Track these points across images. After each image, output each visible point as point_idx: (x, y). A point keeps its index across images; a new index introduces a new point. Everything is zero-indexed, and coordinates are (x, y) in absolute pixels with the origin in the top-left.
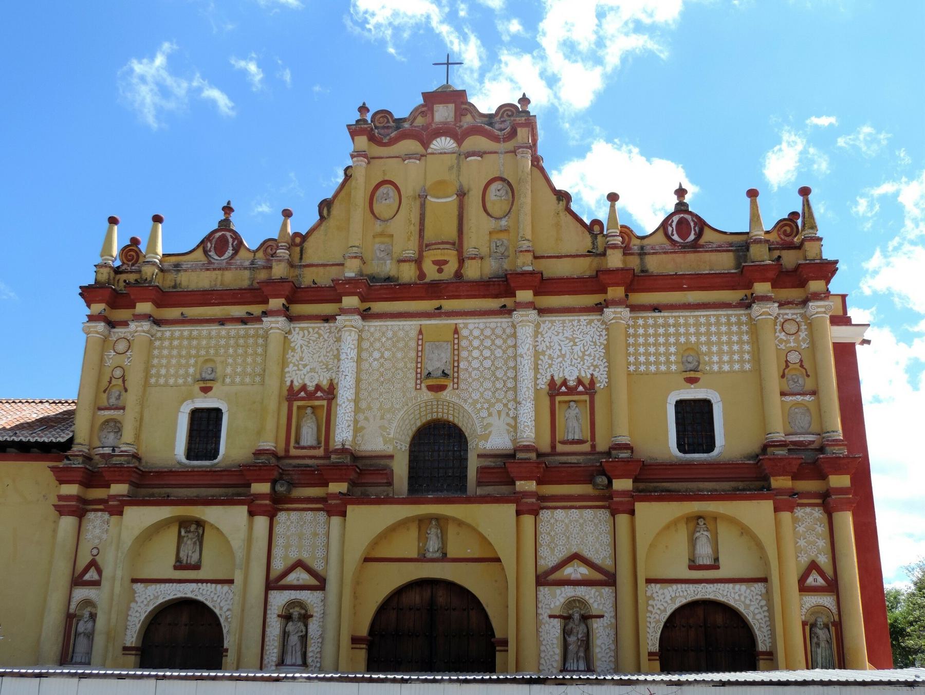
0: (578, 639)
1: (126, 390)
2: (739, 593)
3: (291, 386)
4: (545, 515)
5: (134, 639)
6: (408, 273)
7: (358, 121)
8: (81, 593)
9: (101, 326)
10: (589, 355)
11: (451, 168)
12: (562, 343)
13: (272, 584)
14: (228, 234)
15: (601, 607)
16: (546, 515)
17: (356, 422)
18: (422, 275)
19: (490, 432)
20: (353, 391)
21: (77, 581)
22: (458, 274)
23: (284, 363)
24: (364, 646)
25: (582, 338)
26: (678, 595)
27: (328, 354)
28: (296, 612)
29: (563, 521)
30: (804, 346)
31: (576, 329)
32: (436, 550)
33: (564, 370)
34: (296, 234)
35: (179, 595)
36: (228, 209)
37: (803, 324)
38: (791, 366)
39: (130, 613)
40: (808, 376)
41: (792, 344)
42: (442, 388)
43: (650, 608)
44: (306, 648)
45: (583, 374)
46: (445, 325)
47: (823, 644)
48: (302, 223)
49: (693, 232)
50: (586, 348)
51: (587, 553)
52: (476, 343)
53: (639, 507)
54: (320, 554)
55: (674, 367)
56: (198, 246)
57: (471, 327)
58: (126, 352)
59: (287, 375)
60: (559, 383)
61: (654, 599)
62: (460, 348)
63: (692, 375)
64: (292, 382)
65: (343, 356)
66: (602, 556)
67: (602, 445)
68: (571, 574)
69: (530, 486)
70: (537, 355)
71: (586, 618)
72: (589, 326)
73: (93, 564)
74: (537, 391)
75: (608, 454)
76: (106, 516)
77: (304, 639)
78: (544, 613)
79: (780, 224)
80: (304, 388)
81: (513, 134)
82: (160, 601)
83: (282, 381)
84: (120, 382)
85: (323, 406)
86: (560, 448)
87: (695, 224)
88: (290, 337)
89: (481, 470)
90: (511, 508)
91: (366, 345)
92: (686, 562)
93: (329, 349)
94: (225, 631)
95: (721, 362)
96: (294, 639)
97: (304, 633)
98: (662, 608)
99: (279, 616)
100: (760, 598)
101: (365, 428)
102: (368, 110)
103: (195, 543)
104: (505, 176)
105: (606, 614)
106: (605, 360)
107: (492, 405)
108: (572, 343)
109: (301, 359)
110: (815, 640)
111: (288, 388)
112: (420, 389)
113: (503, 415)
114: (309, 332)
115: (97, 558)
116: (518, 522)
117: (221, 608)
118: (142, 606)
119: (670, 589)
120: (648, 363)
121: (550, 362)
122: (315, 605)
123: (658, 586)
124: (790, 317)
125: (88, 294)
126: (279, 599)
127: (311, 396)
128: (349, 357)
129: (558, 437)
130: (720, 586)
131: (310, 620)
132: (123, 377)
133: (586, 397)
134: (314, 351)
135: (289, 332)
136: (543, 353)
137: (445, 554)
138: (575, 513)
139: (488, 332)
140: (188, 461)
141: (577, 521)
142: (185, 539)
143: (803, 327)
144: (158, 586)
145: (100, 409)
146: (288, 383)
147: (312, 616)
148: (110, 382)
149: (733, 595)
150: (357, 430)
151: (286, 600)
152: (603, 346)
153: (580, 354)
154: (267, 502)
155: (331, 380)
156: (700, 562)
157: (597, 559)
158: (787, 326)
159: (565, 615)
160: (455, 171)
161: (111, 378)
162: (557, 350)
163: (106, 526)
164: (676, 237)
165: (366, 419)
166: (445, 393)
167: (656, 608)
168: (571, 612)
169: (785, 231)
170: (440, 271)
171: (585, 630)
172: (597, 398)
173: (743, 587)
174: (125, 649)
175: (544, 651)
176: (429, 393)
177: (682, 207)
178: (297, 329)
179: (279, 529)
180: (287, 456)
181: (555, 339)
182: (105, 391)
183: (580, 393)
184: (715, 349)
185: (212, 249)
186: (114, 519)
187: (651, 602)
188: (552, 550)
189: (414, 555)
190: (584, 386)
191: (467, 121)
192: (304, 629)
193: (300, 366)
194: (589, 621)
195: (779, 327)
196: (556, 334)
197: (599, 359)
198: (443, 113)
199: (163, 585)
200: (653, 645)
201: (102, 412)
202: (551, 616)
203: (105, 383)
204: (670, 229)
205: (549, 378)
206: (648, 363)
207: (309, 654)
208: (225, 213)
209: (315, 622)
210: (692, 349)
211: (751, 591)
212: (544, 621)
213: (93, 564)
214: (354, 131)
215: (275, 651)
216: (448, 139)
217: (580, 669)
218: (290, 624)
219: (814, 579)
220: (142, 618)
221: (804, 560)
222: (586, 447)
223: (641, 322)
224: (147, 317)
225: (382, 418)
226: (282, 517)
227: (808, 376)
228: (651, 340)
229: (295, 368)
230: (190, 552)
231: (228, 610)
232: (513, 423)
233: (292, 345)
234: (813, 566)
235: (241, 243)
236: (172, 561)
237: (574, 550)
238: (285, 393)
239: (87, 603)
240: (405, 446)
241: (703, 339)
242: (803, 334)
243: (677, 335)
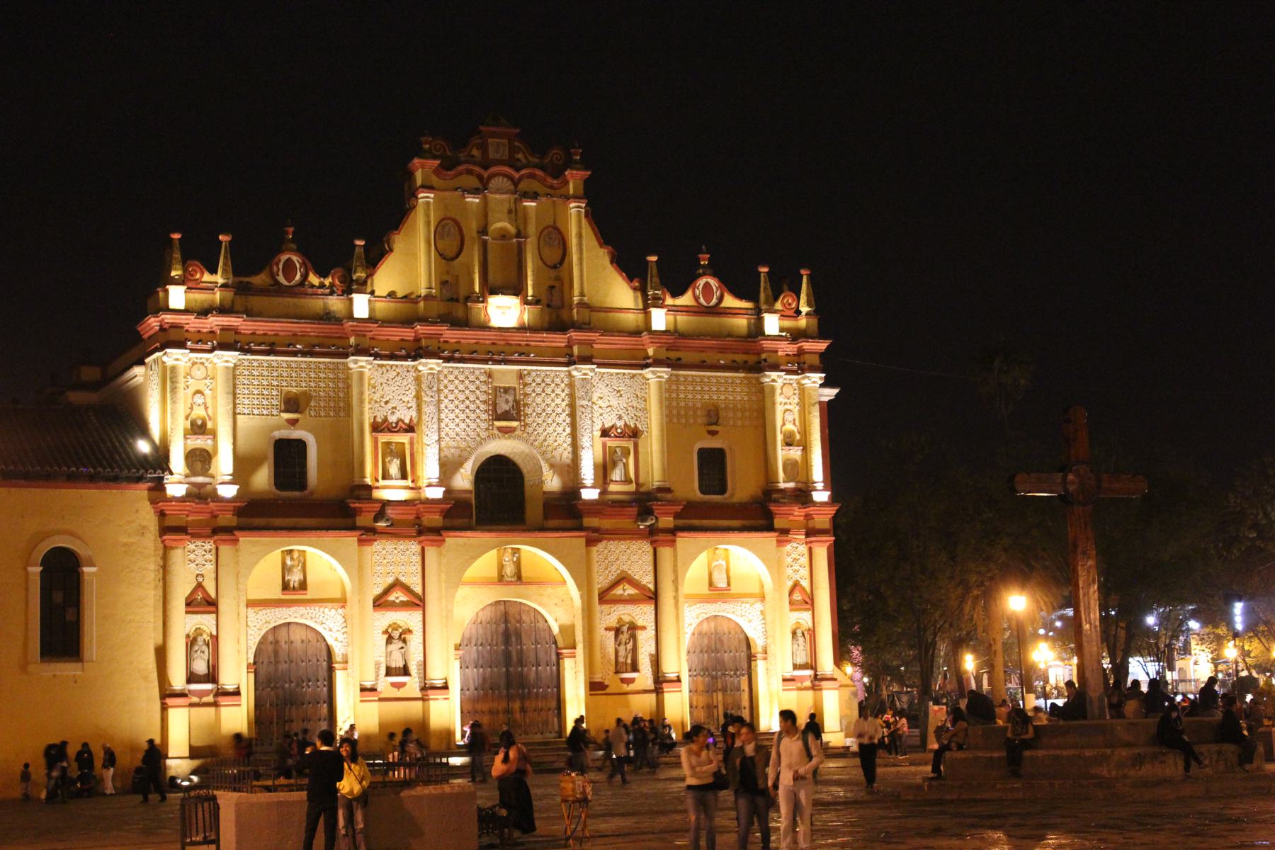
11: (510, 212)
14: (295, 258)
20: (437, 434)
27: (407, 393)
46: (512, 371)
49: (715, 297)
54: (418, 579)
63: (714, 428)
108: (618, 395)
118: (255, 629)
140: (278, 492)
147: (410, 631)
148: (192, 408)
160: (513, 215)
161: (192, 405)
164: (702, 300)
185: (280, 273)
193: (383, 404)
204: (697, 292)
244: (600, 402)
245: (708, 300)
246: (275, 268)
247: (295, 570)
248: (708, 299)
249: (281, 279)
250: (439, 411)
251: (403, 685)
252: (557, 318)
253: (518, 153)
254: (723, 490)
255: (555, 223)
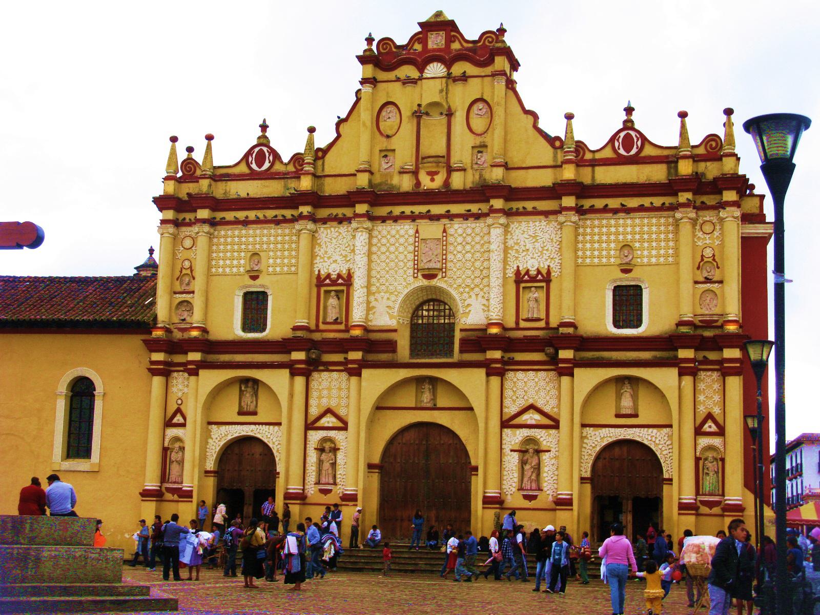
0: (532, 467)
1: (194, 278)
2: (652, 435)
3: (319, 275)
4: (510, 375)
5: (212, 465)
6: (406, 184)
7: (365, 51)
8: (172, 432)
9: (171, 229)
10: (547, 250)
11: (441, 91)
12: (526, 241)
13: (310, 426)
14: (265, 149)
15: (548, 444)
16: (510, 375)
17: (368, 302)
18: (418, 184)
19: (470, 311)
21: (169, 423)
22: (447, 183)
23: (313, 256)
24: (377, 471)
25: (542, 237)
26: (605, 436)
27: (346, 249)
28: (327, 445)
29: (523, 380)
30: (717, 242)
31: (538, 229)
32: (429, 401)
33: (527, 262)
34: (319, 149)
35: (243, 433)
36: (264, 127)
37: (718, 225)
38: (706, 260)
39: (208, 447)
40: (718, 268)
41: (708, 242)
42: (433, 276)
43: (584, 445)
44: (335, 472)
45: (542, 266)
47: (711, 474)
48: (322, 140)
49: (635, 146)
50: (545, 244)
51: (539, 404)
52: (460, 240)
53: (577, 371)
55: (612, 260)
56: (242, 160)
57: (456, 226)
58: (192, 247)
59: (316, 266)
60: (523, 273)
61: (588, 439)
62: (448, 244)
64: (319, 271)
65: (357, 252)
66: (551, 407)
67: (554, 323)
68: (527, 419)
69: (497, 354)
70: (506, 250)
71: (538, 452)
72: (548, 226)
73: (178, 411)
74: (505, 278)
75: (557, 329)
76: (186, 375)
77: (334, 465)
78: (507, 448)
79: (708, 139)
80: (328, 276)
81: (490, 61)
82: (229, 437)
83: (312, 272)
84: (189, 272)
85: (343, 291)
86: (523, 324)
87: (638, 140)
88: (316, 235)
89: (463, 341)
90: (482, 372)
91: (375, 241)
92: (613, 412)
93: (346, 245)
94: (277, 459)
95: (650, 256)
96: (326, 465)
97: (334, 461)
98: (593, 445)
99: (315, 449)
100: (666, 438)
101: (375, 307)
102: (373, 40)
103: (252, 396)
104: (485, 98)
105: (552, 449)
106: (559, 254)
107: (473, 289)
109: (326, 252)
110: (706, 471)
111: (316, 276)
112: (417, 277)
113: (480, 297)
114: (331, 232)
115: (182, 407)
116: (488, 382)
117: (274, 443)
118: (217, 441)
119: (600, 431)
120: (592, 257)
121: (516, 255)
122: (341, 441)
123: (592, 429)
124: (708, 219)
125: (161, 202)
126: (315, 437)
127: (334, 283)
128: (362, 252)
129: (524, 314)
130: (637, 430)
131: (338, 452)
132: (191, 267)
133: (544, 284)
134: (336, 247)
135: (316, 231)
136: (512, 248)
137: (435, 405)
138: (531, 374)
139: (469, 231)
141: (533, 380)
142: (245, 393)
143: (718, 227)
144: (227, 426)
145: (175, 293)
146: (317, 273)
147: (339, 449)
148: (181, 272)
149: (646, 436)
150: (369, 309)
151: (320, 437)
152: (558, 243)
153: (540, 249)
154: (303, 366)
155: (349, 270)
156: (623, 412)
157: (547, 409)
158: (704, 228)
159: (523, 449)
160: (444, 93)
161: (181, 269)
162: (522, 246)
163: (186, 383)
164: (622, 151)
165: (376, 300)
166: (435, 280)
167: (589, 445)
168: (527, 447)
169: (711, 145)
170: (432, 180)
171: (537, 461)
172: (552, 285)
173: (655, 430)
174: (207, 472)
175: (506, 475)
176: (424, 280)
177: (628, 125)
178: (322, 229)
179: (314, 384)
180: (317, 330)
181: (522, 237)
182: (177, 279)
183: (540, 281)
184: (646, 245)
185: (254, 162)
186: (193, 378)
187: (586, 441)
188: (514, 401)
189: (413, 405)
190: (542, 275)
191: (456, 46)
192: (333, 457)
194: (541, 454)
195: (698, 227)
196: (522, 232)
197: (554, 253)
198: (436, 41)
199: (230, 426)
200: (586, 472)
201: (177, 295)
202: (512, 451)
203: (177, 273)
204: (616, 144)
205: (515, 268)
206: (592, 257)
207: (338, 476)
208: (262, 131)
209: (341, 453)
210: (629, 245)
211: (661, 433)
212: (506, 454)
213: (178, 411)
214: (363, 60)
215: (314, 473)
216: (439, 64)
217: (533, 488)
218: (324, 455)
219: (710, 427)
220: (217, 450)
221: (702, 410)
222: (542, 324)
223: (588, 222)
224: (204, 221)
225: (388, 299)
226: (315, 375)
227: (718, 268)
228: (596, 238)
229: (322, 260)
230: (249, 402)
231: (279, 444)
232: (485, 302)
233: (319, 242)
234: (710, 416)
235: (276, 156)
236: (237, 410)
237: (531, 401)
238: (315, 281)
239: (177, 439)
240: (407, 321)
241: (637, 237)
242: (716, 234)
243: (617, 234)
244: (516, 247)
245: (628, 148)
246: (250, 159)
247: (248, 395)
248: (628, 148)
249: (254, 166)
250: (370, 261)
251: (330, 491)
252: (480, 178)
253: (454, 42)
254: (638, 323)
255: (482, 96)
